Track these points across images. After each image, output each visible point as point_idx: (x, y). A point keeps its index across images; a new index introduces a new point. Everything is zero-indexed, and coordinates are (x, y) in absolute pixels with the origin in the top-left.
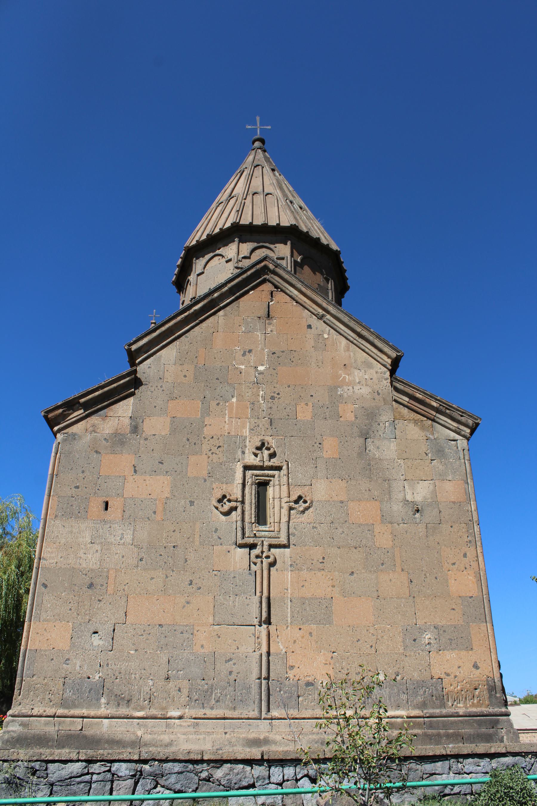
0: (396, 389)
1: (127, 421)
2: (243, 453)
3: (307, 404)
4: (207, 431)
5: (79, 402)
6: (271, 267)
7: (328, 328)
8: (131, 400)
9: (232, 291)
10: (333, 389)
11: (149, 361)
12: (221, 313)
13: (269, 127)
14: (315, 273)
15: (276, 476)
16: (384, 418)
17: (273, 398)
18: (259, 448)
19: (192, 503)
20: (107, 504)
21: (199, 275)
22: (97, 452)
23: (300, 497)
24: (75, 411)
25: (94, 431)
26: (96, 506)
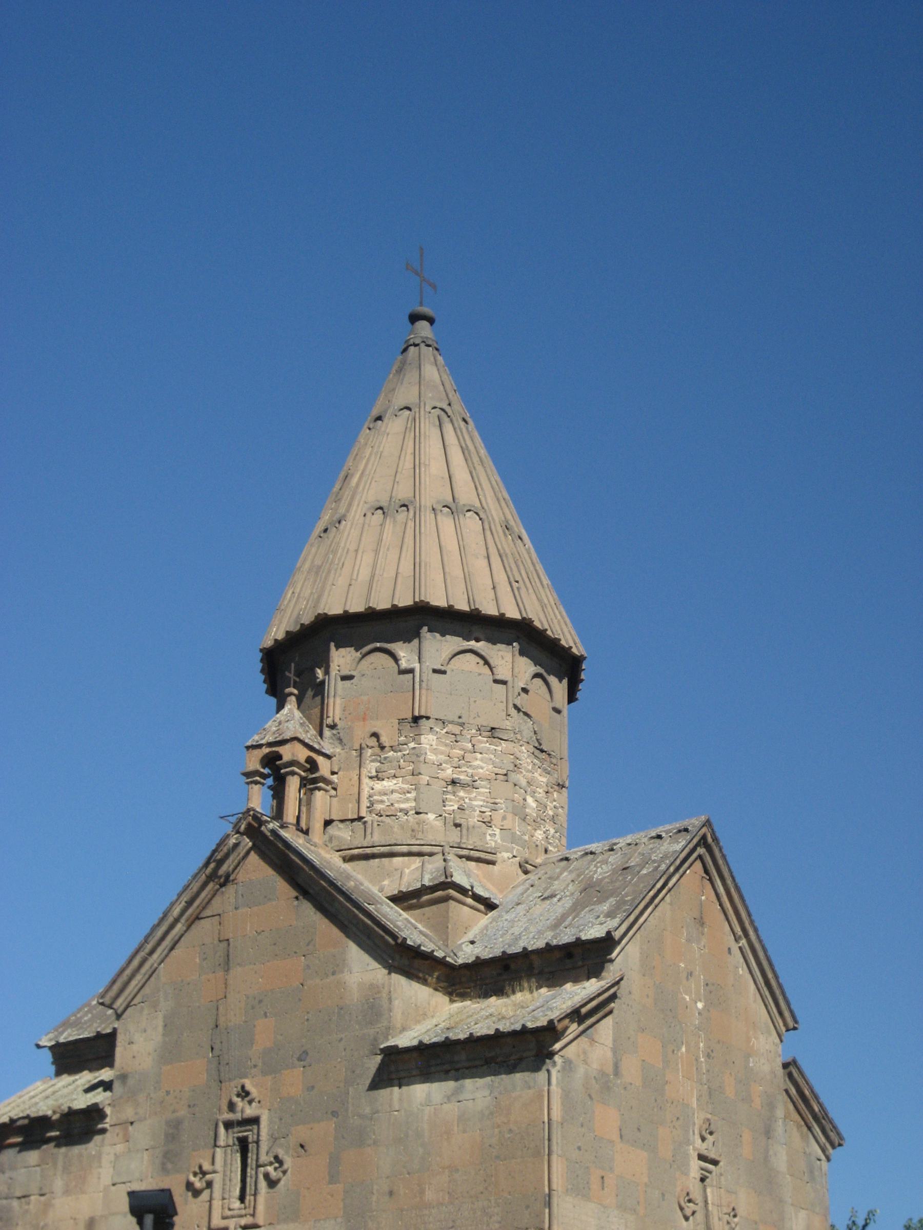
0: (790, 1075)
1: (609, 1054)
2: (694, 1134)
3: (730, 1073)
6: (710, 840)
7: (742, 960)
8: (609, 1020)
10: (748, 1056)
12: (668, 898)
15: (714, 1174)
17: (708, 1056)
19: (663, 1195)
20: (603, 1178)
21: (435, 671)
22: (590, 1096)
23: (734, 1209)
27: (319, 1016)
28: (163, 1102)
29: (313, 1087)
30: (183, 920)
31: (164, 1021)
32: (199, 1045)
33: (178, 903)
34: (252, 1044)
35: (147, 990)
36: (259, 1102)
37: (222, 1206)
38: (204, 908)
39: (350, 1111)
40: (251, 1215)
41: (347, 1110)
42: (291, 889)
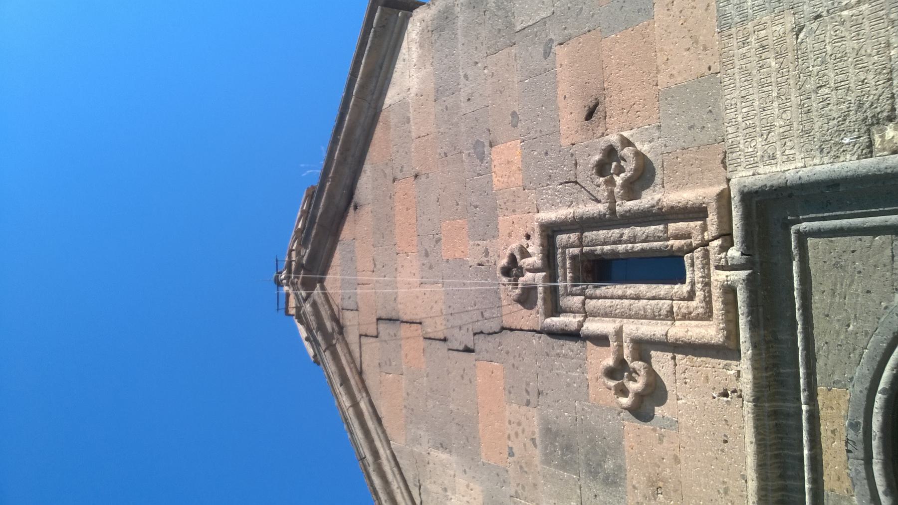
27: (442, 133)
28: (521, 467)
29: (514, 114)
30: (358, 396)
31: (438, 449)
32: (462, 377)
33: (340, 396)
34: (465, 262)
35: (409, 476)
36: (528, 237)
37: (686, 317)
38: (354, 362)
39: (544, 15)
40: (704, 229)
41: (544, 21)
42: (348, 219)
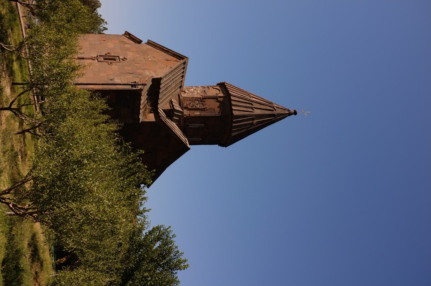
1: (128, 42)
4: (128, 52)
5: (130, 35)
8: (134, 43)
9: (174, 54)
10: (147, 69)
11: (146, 45)
12: (166, 54)
13: (306, 115)
14: (218, 107)
16: (139, 76)
18: (124, 58)
19: (107, 50)
20: (105, 41)
24: (128, 36)
25: (124, 39)
26: (104, 40)
